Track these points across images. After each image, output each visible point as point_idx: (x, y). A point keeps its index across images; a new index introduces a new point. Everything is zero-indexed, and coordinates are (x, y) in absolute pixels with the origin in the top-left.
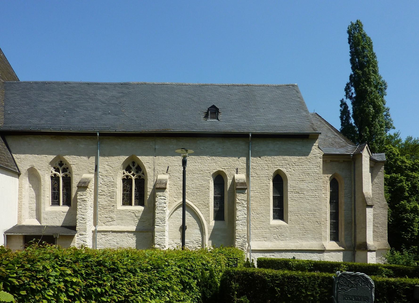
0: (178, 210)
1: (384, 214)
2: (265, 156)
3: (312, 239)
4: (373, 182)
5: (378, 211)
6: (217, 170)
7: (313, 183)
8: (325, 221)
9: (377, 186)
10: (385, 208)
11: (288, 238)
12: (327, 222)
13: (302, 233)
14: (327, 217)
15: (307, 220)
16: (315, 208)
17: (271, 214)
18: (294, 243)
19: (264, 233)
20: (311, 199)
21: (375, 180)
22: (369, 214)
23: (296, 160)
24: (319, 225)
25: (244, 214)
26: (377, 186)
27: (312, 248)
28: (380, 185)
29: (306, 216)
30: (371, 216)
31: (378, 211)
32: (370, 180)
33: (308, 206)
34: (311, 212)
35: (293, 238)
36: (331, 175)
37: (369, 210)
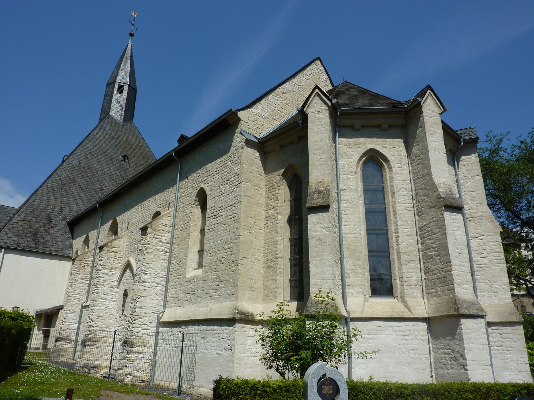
0: (126, 272)
1: (439, 221)
2: (191, 174)
3: (226, 298)
4: (412, 156)
5: (428, 218)
6: (155, 212)
7: (233, 193)
8: (274, 260)
9: (419, 160)
10: (440, 206)
11: (199, 299)
12: (277, 261)
13: (215, 287)
14: (276, 251)
15: (222, 262)
16: (232, 236)
17: (189, 261)
18: (204, 307)
19: (179, 292)
20: (229, 222)
21: (414, 150)
22: (317, 226)
23: (217, 166)
24: (235, 268)
25: (142, 265)
26: (419, 160)
27: (220, 315)
28: (422, 156)
29: (222, 255)
30: (323, 230)
31: (428, 218)
32: (404, 152)
33: (225, 236)
34: (228, 245)
35: (204, 297)
36: (282, 171)
37: (316, 217)
